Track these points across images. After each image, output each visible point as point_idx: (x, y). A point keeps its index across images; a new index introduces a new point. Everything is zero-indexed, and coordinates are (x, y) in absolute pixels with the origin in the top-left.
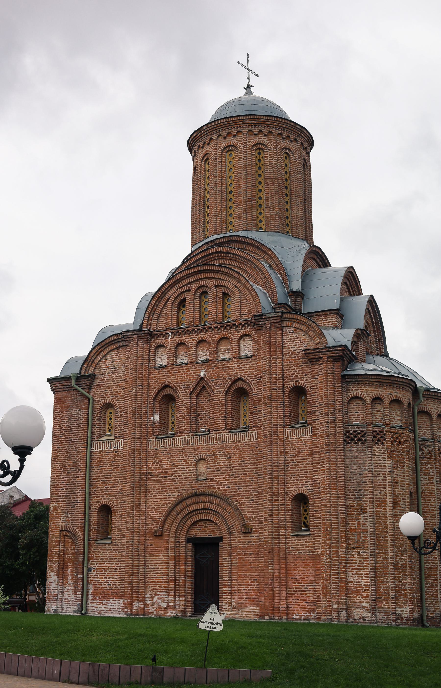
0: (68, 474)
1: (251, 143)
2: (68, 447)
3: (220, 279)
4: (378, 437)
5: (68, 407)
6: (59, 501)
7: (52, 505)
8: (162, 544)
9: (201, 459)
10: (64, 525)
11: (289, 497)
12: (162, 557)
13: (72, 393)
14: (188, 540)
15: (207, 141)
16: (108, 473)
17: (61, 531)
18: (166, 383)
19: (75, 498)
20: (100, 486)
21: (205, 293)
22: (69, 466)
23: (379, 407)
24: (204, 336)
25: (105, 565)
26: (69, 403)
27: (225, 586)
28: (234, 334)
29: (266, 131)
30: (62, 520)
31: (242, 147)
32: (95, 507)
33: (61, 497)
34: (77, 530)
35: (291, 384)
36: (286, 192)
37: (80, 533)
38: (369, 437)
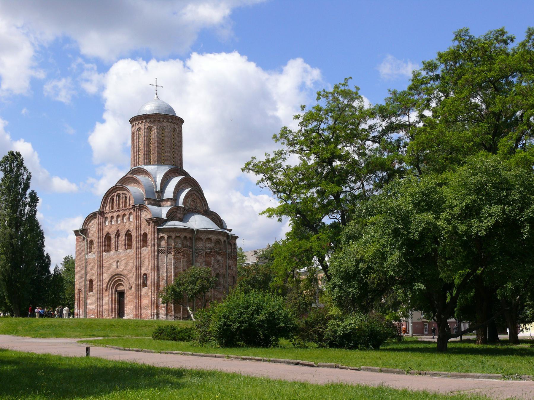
1: (146, 126)
4: (169, 251)
8: (107, 293)
9: (118, 261)
11: (142, 275)
12: (107, 298)
14: (116, 291)
20: (89, 272)
21: (119, 196)
23: (171, 239)
28: (127, 213)
29: (152, 120)
31: (143, 128)
32: (88, 280)
35: (143, 232)
36: (163, 145)
38: (166, 251)
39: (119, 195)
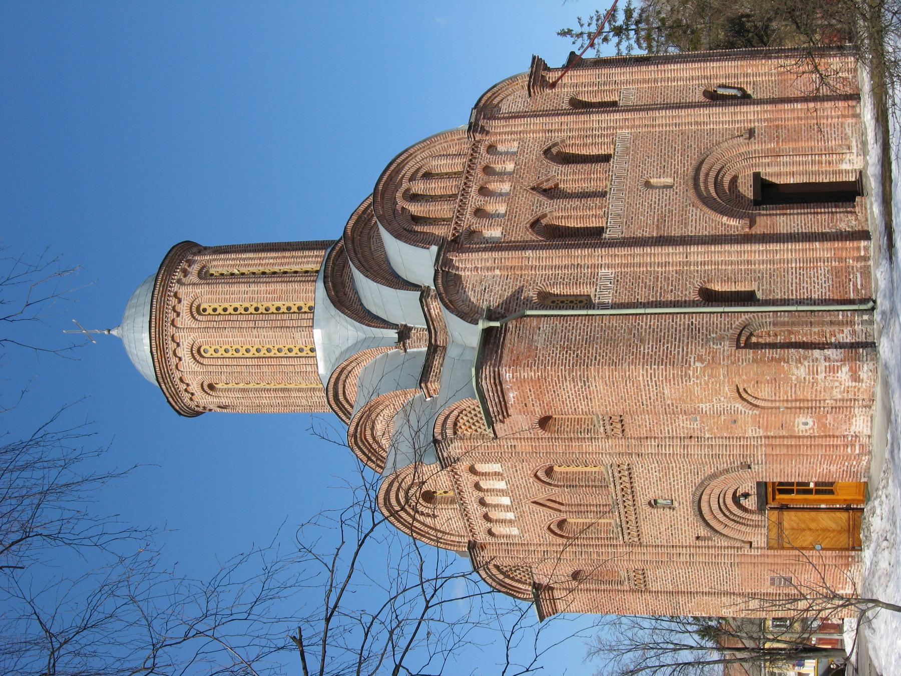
0: (642, 341)
2: (597, 343)
3: (403, 176)
5: (529, 348)
6: (687, 352)
7: (692, 364)
10: (727, 343)
13: (507, 341)
15: (173, 301)
16: (649, 290)
17: (738, 347)
18: (528, 226)
19: (684, 329)
22: (629, 340)
24: (473, 190)
25: (794, 288)
26: (523, 347)
27: (820, 162)
28: (484, 158)
30: (719, 346)
33: (681, 350)
34: (737, 323)
37: (743, 317)
39: (414, 198)
